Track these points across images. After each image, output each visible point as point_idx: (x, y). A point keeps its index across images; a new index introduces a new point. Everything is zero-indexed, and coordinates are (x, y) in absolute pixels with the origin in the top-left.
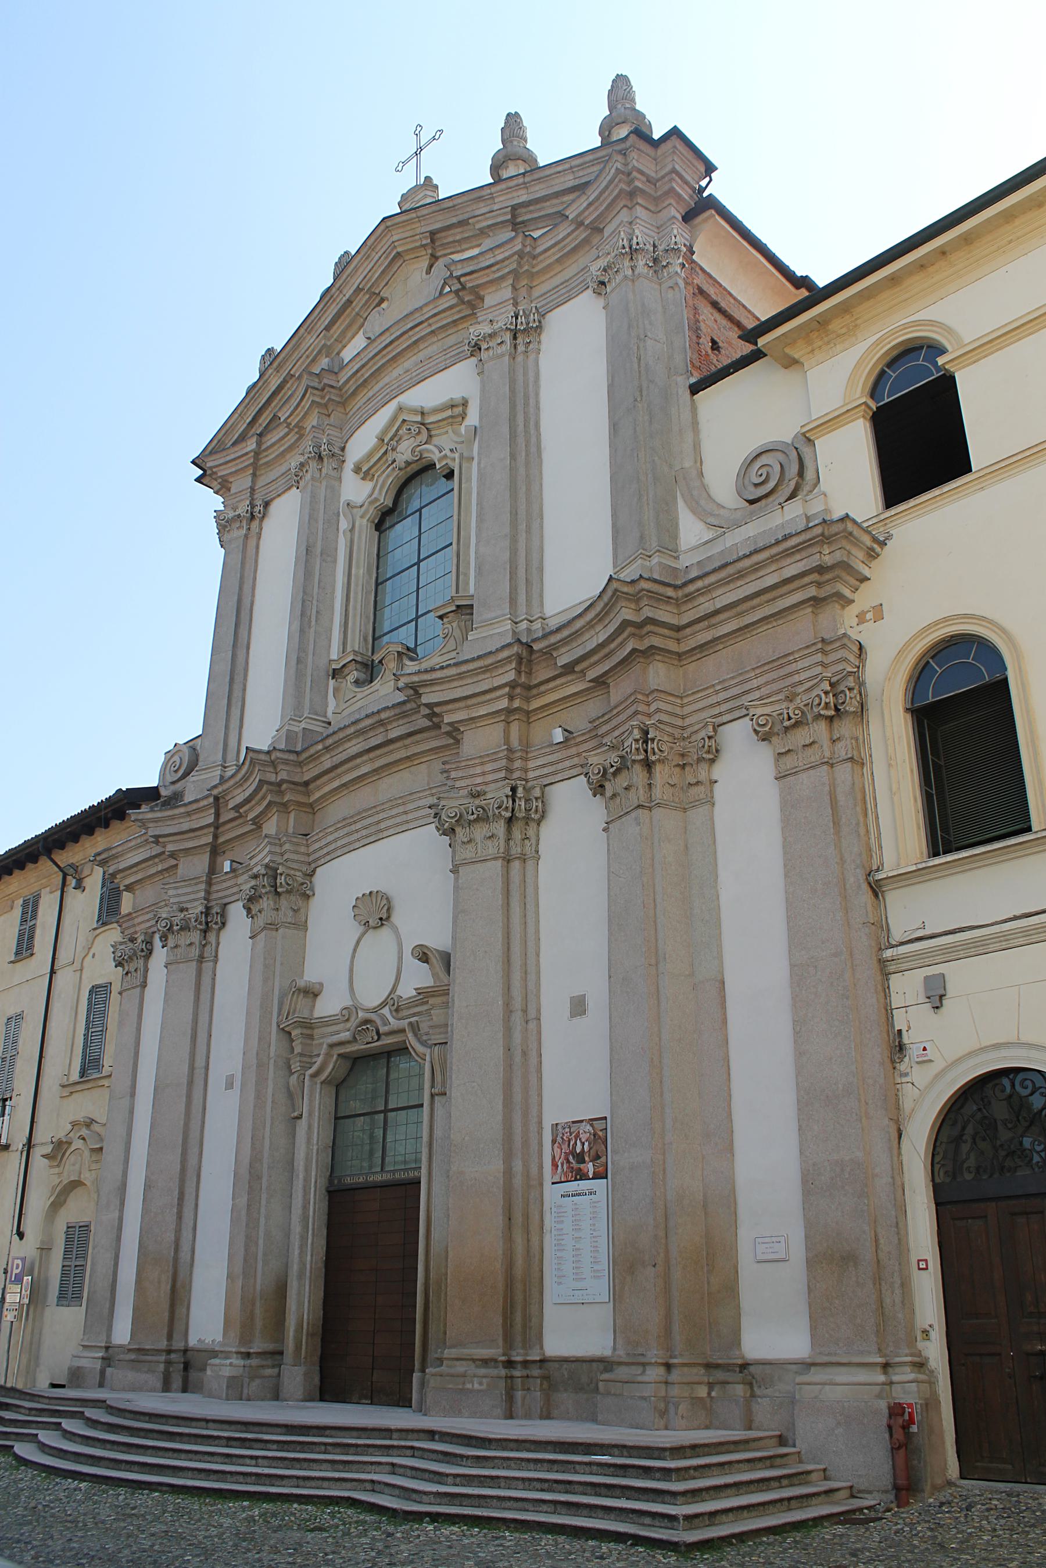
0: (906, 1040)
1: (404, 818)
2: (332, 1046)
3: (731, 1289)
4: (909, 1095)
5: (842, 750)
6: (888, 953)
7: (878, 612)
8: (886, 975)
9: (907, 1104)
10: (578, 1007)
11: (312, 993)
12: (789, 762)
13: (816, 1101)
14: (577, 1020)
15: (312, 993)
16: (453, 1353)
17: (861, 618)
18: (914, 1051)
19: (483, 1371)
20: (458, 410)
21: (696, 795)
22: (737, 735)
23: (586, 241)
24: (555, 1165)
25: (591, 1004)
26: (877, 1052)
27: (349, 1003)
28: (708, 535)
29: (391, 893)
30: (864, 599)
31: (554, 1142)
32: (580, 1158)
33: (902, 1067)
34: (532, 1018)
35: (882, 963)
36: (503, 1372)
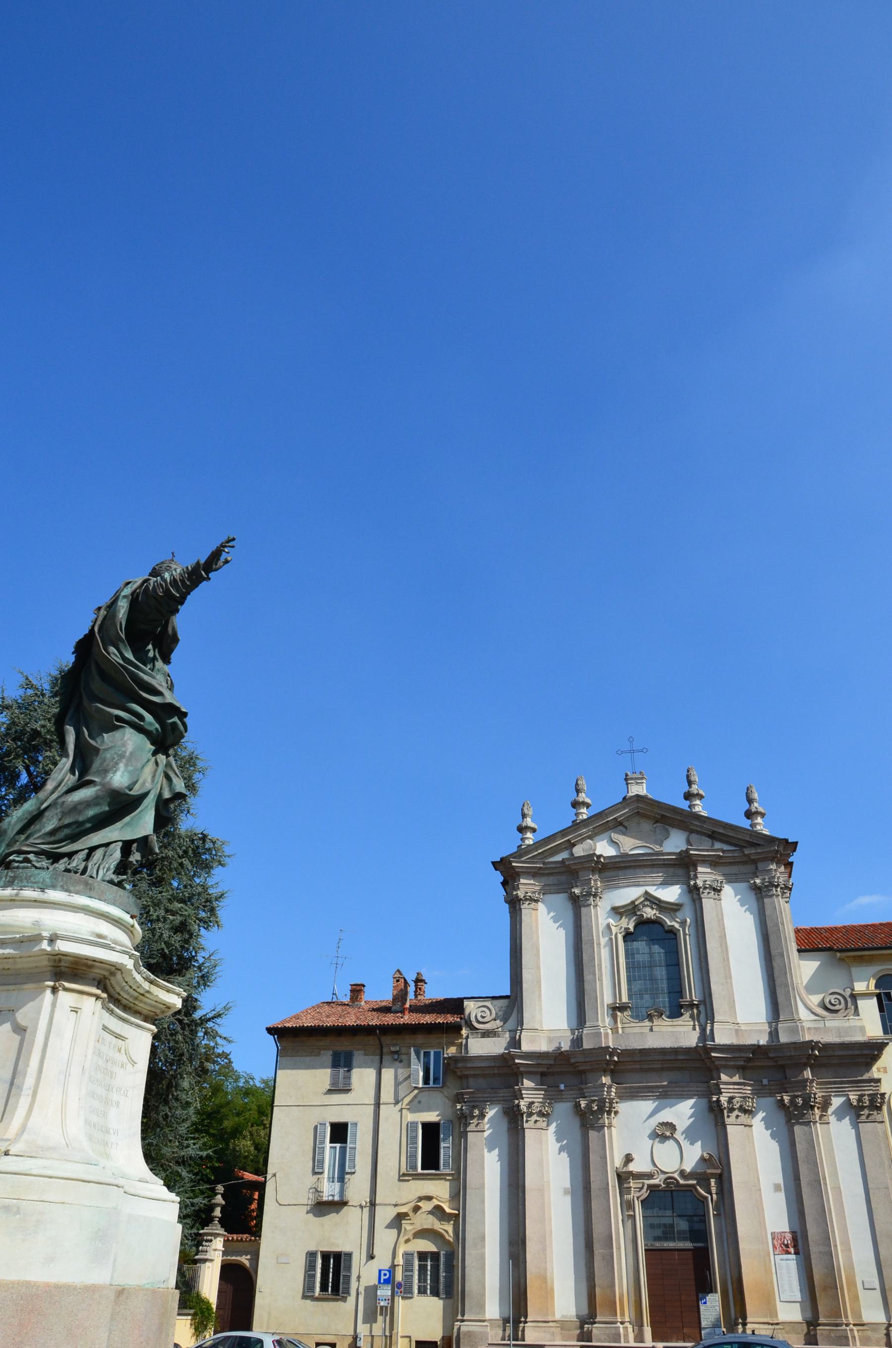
7: (885, 1070)
17: (879, 1070)
24: (774, 1247)
30: (879, 1064)
31: (773, 1239)
32: (787, 1246)
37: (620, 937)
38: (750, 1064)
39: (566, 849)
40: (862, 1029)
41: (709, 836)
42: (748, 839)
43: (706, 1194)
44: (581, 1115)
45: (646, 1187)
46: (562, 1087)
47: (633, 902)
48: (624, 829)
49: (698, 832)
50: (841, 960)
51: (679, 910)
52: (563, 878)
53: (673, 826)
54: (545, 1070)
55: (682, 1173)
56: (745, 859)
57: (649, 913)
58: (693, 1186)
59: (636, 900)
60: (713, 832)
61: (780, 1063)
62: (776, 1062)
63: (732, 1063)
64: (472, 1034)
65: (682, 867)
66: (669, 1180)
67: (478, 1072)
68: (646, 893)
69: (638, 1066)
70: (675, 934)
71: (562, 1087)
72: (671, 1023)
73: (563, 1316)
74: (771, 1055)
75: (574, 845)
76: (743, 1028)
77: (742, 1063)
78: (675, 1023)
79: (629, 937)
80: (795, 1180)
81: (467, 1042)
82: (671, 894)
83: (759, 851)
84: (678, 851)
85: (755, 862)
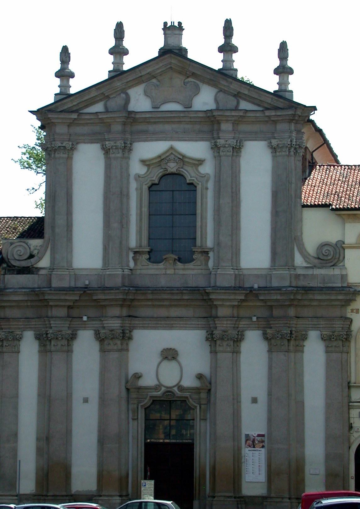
0: (353, 425)
1: (185, 326)
2: (151, 397)
3: (303, 480)
4: (352, 439)
5: (345, 349)
6: (351, 404)
8: (349, 409)
9: (352, 441)
10: (255, 400)
11: (138, 376)
12: (330, 349)
13: (329, 438)
14: (254, 404)
15: (138, 376)
16: (219, 494)
18: (353, 429)
19: (229, 499)
20: (200, 162)
21: (300, 349)
22: (313, 335)
23: (267, 121)
25: (259, 400)
26: (347, 428)
27: (157, 383)
28: (305, 265)
29: (177, 349)
33: (351, 432)
34: (239, 402)
35: (349, 406)
36: (233, 499)
37: (145, 188)
38: (244, 304)
39: (101, 100)
40: (344, 277)
41: (235, 96)
42: (269, 102)
43: (196, 405)
44: (100, 341)
45: (149, 397)
46: (85, 318)
47: (159, 156)
48: (158, 83)
49: (225, 92)
50: (339, 215)
51: (201, 164)
52: (97, 128)
53: (204, 82)
54: (72, 304)
55: (181, 388)
56: (267, 119)
57: (172, 167)
58: (187, 397)
59: (163, 154)
60: (239, 93)
61: (269, 304)
62: (266, 302)
63: (228, 303)
64: (9, 271)
65: (208, 125)
66: (169, 391)
67: (14, 304)
68: (172, 148)
69: (150, 303)
70: (196, 187)
71: (85, 318)
72: (183, 267)
73: (77, 491)
74: (261, 298)
75: (108, 97)
76: (246, 272)
77: (236, 304)
78: (186, 267)
79: (154, 188)
80: (268, 395)
81: (4, 278)
82: (195, 149)
83: (279, 114)
84: (205, 109)
85: (275, 122)
